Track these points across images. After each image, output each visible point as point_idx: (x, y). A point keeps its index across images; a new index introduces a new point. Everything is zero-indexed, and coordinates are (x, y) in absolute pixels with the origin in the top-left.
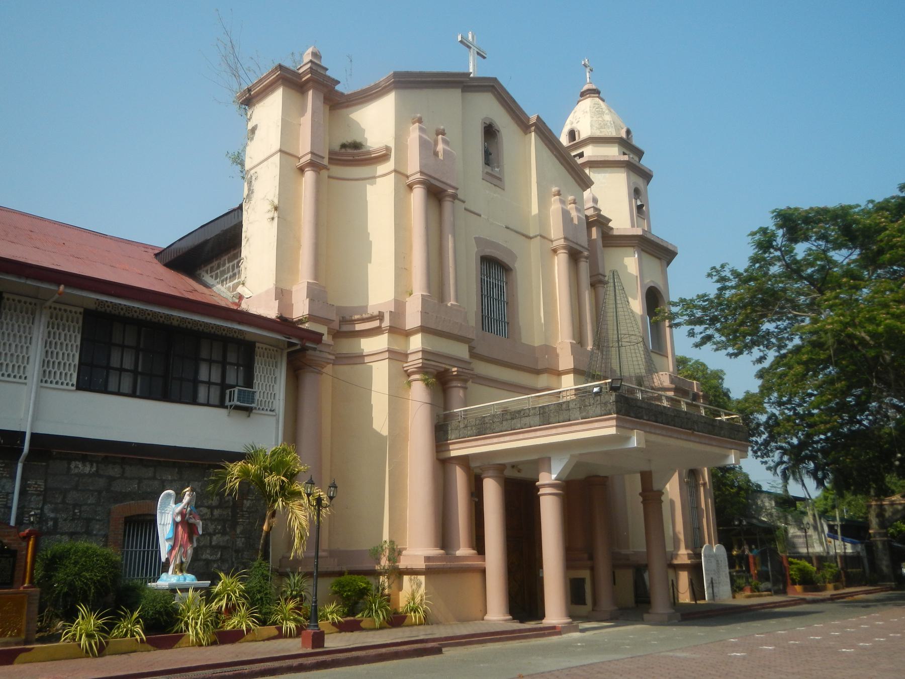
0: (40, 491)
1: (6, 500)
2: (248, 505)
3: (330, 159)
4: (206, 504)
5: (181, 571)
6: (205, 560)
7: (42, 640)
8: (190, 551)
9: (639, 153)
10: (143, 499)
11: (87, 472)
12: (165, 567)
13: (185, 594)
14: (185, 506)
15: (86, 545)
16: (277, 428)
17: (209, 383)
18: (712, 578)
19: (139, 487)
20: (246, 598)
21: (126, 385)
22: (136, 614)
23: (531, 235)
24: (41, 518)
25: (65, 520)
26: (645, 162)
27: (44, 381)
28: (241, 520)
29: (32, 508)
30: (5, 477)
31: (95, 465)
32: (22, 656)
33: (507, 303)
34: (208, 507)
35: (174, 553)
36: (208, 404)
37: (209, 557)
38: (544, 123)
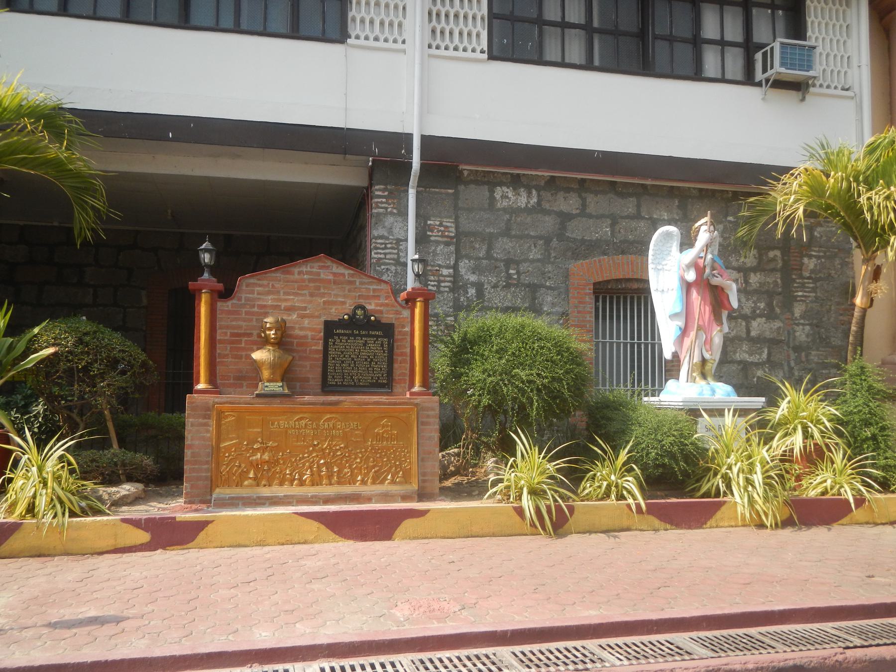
0: (448, 237)
1: (396, 251)
2: (812, 266)
4: (735, 264)
5: (704, 376)
6: (740, 362)
7: (457, 493)
8: (718, 340)
10: (623, 253)
11: (523, 206)
12: (672, 369)
13: (717, 421)
14: (699, 253)
15: (519, 319)
16: (860, 121)
17: (722, 43)
19: (613, 232)
20: (840, 434)
21: (575, 53)
22: (623, 456)
24: (457, 284)
25: (495, 286)
27: (434, 47)
28: (800, 294)
29: (440, 266)
30: (391, 213)
31: (534, 192)
32: (408, 525)
35: (687, 342)
36: (723, 80)
37: (746, 357)
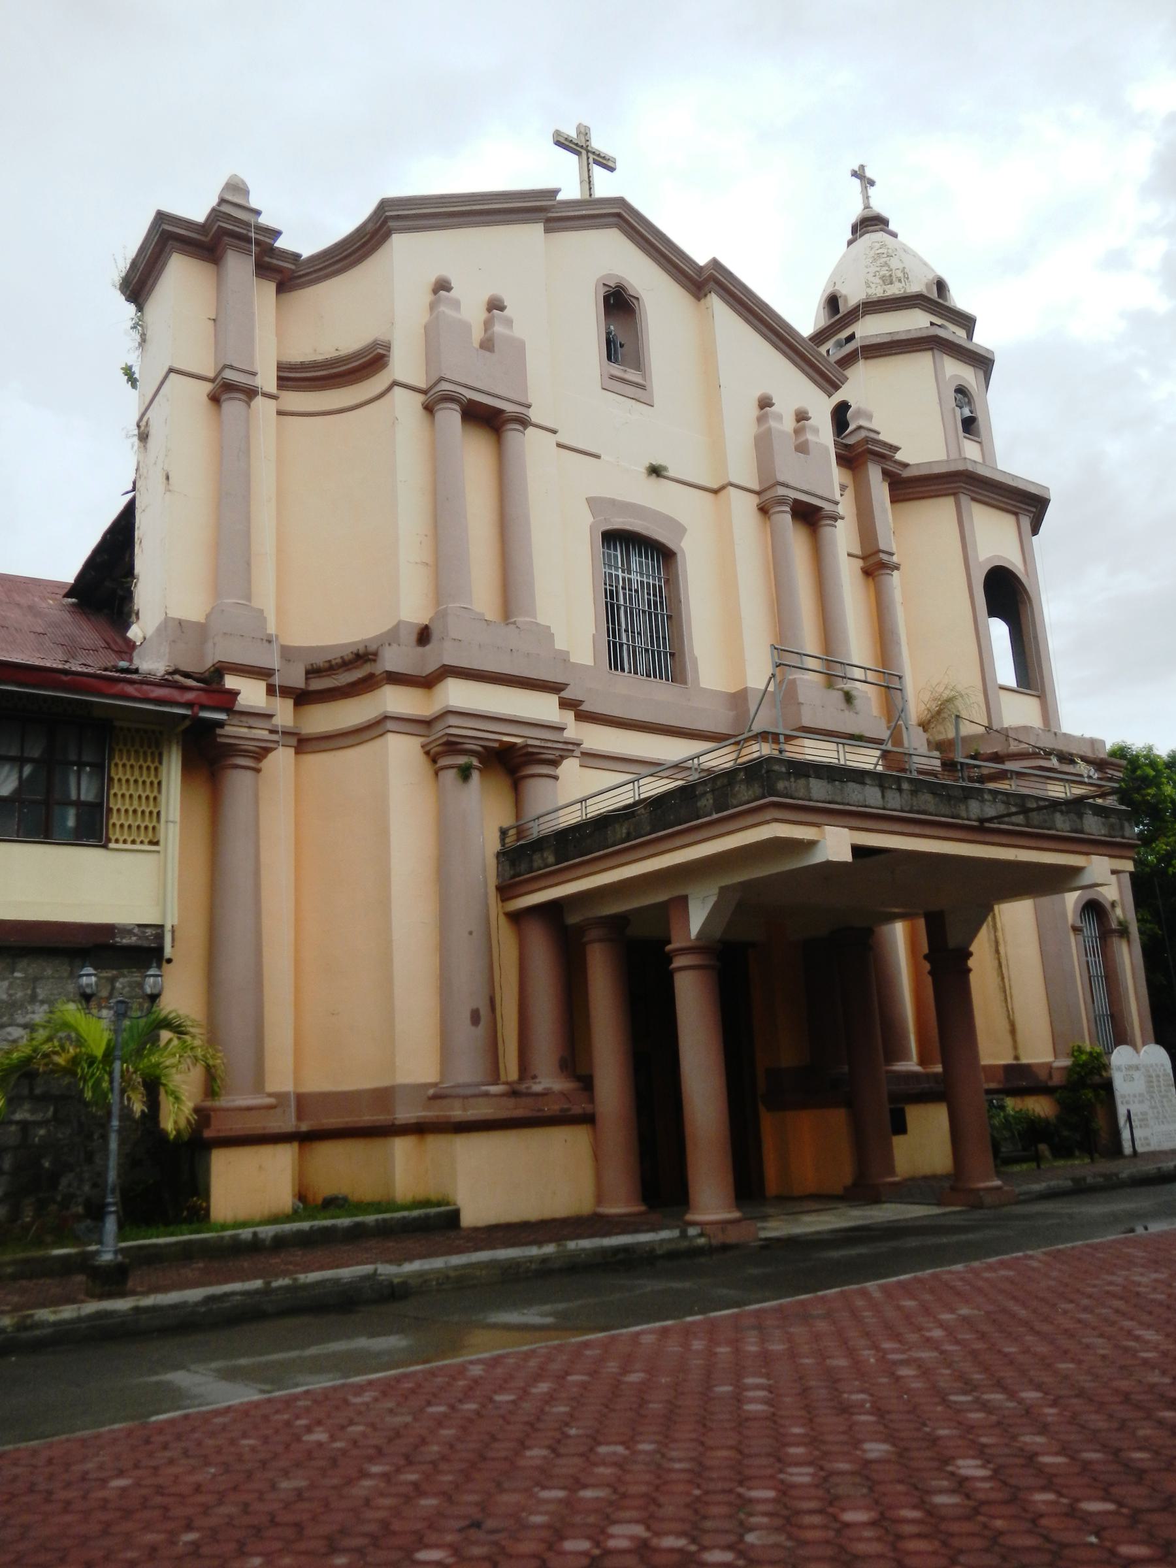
3: (280, 378)
6: (18, 1123)
9: (967, 322)
18: (1129, 1112)
23: (715, 486)
26: (983, 338)
33: (669, 617)
34: (25, 1026)
38: (731, 274)
